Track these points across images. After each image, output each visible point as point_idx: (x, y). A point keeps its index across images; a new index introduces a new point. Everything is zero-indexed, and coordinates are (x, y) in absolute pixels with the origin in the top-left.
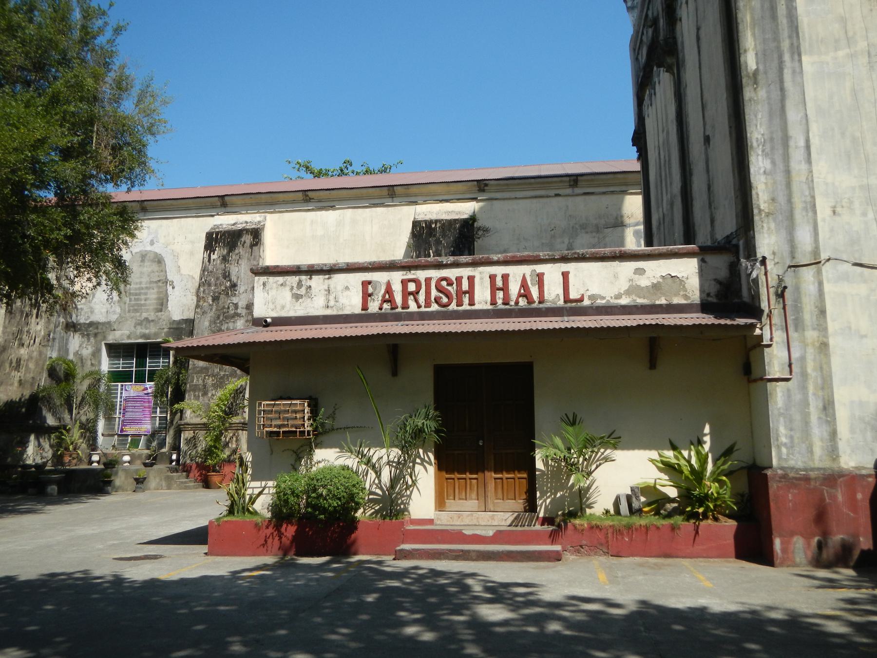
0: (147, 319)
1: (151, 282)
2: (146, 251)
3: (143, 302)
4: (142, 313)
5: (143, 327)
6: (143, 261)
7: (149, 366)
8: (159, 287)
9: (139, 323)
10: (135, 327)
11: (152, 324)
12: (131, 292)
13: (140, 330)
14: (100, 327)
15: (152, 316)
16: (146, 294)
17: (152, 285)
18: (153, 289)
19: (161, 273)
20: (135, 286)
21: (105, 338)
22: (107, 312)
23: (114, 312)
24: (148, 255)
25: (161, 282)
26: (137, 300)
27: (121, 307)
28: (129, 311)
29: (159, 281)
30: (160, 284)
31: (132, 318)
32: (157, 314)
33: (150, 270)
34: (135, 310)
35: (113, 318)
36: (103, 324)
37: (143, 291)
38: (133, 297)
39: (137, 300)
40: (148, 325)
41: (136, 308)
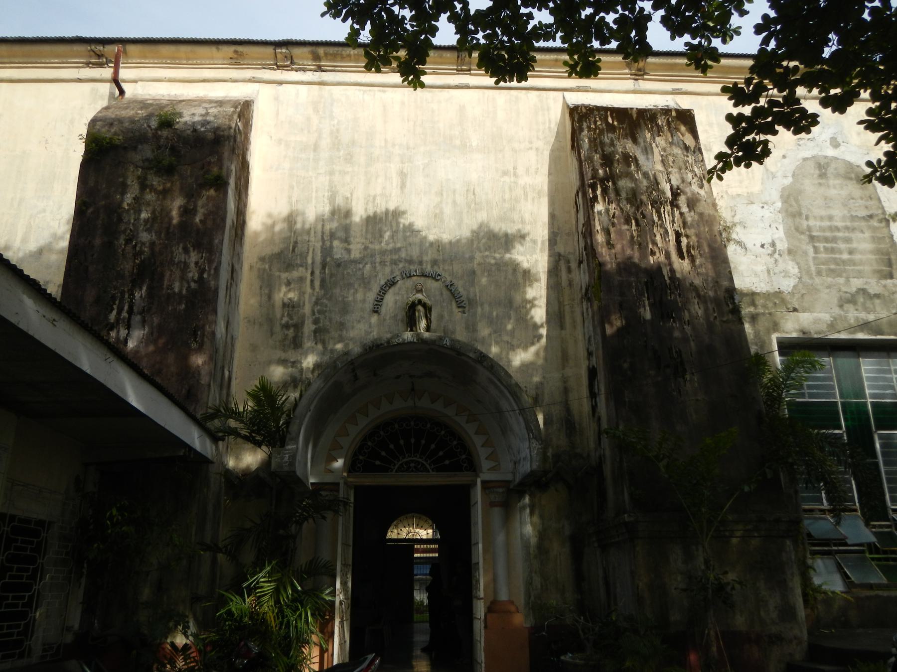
0: (863, 291)
1: (853, 218)
2: (826, 157)
3: (845, 256)
4: (848, 279)
5: (860, 308)
6: (823, 175)
7: (873, 396)
8: (874, 229)
9: (851, 300)
10: (841, 306)
11: (877, 301)
12: (814, 234)
13: (853, 315)
14: (760, 301)
15: (874, 287)
16: (848, 240)
17: (856, 224)
18: (862, 232)
19: (870, 203)
20: (818, 223)
21: (776, 327)
22: (769, 271)
23: (786, 274)
24: (833, 165)
25: (876, 219)
26: (832, 251)
27: (798, 264)
28: (819, 273)
29: (871, 217)
30: (875, 223)
31: (829, 287)
32: (883, 282)
33: (844, 193)
34: (832, 271)
35: (787, 285)
36: (767, 296)
37: (840, 234)
38: (821, 245)
39: (832, 251)
40: (869, 304)
41: (833, 267)
